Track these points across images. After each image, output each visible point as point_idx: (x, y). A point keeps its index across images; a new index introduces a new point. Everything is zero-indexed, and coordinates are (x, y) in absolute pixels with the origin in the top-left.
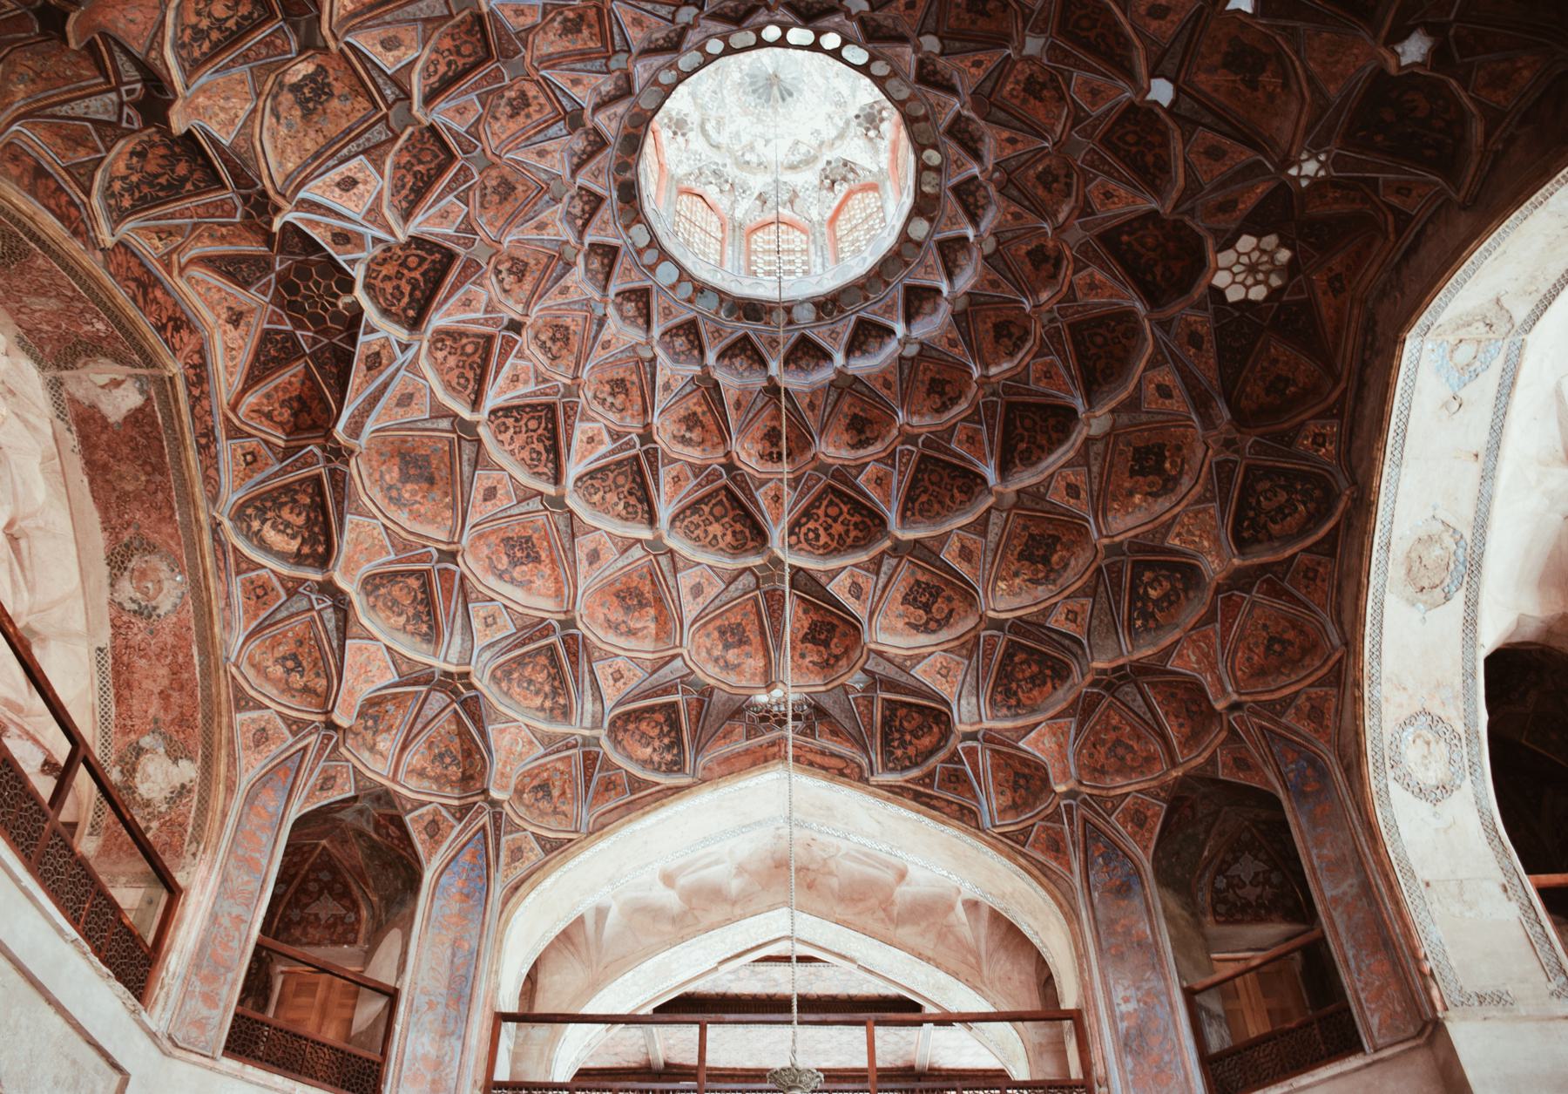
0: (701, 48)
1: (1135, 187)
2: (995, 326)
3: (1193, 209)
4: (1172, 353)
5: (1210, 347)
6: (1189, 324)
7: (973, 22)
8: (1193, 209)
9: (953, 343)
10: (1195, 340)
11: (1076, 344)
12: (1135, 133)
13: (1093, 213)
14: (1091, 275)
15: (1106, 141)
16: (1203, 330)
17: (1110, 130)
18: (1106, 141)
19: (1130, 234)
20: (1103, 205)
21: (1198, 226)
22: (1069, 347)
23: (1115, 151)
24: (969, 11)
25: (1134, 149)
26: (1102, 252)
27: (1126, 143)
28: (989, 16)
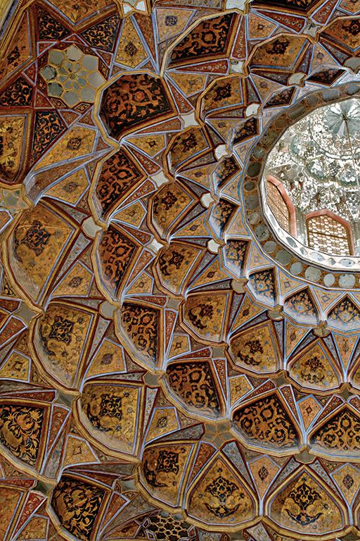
0: (336, 285)
1: (132, 150)
2: (282, 52)
3: (98, 149)
4: (152, 50)
5: (122, 43)
6: (131, 60)
7: (183, 250)
8: (98, 149)
9: (320, 56)
10: (131, 50)
11: (227, 40)
12: (119, 178)
13: (167, 134)
14: (190, 91)
15: (138, 174)
16: (125, 55)
17: (133, 183)
18: (138, 174)
19: (151, 106)
20: (158, 139)
21: (100, 127)
22: (233, 41)
23: (136, 171)
24: (183, 257)
25: (124, 168)
26: (173, 103)
27: (127, 172)
28: (173, 253)
